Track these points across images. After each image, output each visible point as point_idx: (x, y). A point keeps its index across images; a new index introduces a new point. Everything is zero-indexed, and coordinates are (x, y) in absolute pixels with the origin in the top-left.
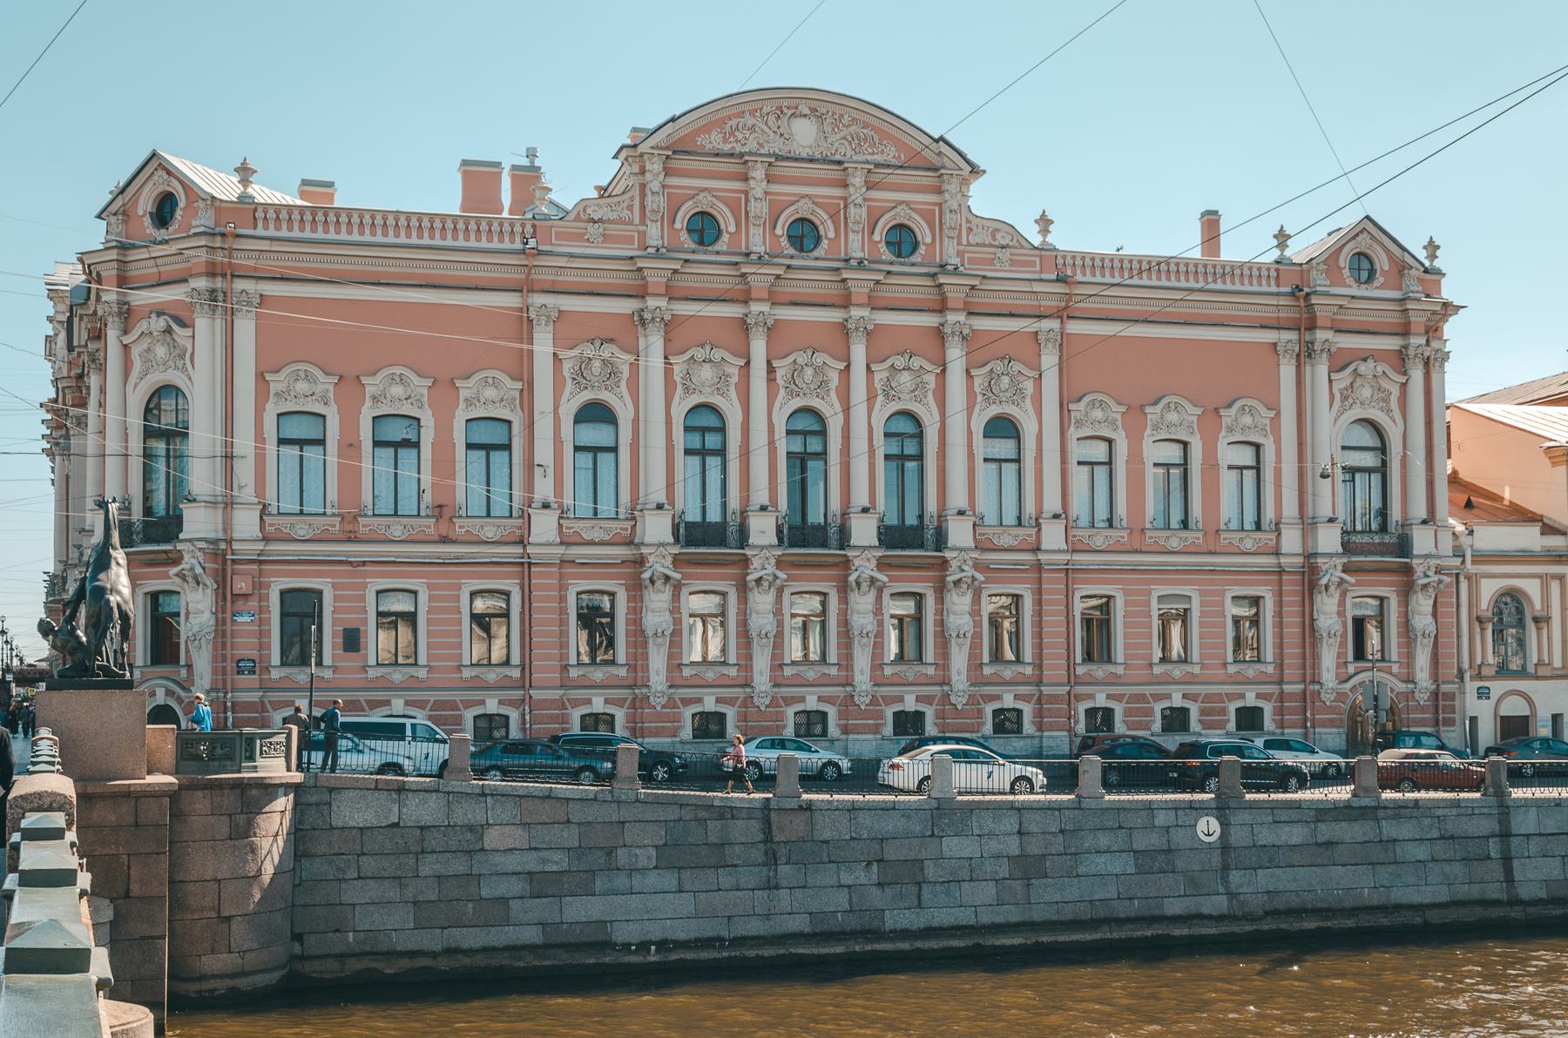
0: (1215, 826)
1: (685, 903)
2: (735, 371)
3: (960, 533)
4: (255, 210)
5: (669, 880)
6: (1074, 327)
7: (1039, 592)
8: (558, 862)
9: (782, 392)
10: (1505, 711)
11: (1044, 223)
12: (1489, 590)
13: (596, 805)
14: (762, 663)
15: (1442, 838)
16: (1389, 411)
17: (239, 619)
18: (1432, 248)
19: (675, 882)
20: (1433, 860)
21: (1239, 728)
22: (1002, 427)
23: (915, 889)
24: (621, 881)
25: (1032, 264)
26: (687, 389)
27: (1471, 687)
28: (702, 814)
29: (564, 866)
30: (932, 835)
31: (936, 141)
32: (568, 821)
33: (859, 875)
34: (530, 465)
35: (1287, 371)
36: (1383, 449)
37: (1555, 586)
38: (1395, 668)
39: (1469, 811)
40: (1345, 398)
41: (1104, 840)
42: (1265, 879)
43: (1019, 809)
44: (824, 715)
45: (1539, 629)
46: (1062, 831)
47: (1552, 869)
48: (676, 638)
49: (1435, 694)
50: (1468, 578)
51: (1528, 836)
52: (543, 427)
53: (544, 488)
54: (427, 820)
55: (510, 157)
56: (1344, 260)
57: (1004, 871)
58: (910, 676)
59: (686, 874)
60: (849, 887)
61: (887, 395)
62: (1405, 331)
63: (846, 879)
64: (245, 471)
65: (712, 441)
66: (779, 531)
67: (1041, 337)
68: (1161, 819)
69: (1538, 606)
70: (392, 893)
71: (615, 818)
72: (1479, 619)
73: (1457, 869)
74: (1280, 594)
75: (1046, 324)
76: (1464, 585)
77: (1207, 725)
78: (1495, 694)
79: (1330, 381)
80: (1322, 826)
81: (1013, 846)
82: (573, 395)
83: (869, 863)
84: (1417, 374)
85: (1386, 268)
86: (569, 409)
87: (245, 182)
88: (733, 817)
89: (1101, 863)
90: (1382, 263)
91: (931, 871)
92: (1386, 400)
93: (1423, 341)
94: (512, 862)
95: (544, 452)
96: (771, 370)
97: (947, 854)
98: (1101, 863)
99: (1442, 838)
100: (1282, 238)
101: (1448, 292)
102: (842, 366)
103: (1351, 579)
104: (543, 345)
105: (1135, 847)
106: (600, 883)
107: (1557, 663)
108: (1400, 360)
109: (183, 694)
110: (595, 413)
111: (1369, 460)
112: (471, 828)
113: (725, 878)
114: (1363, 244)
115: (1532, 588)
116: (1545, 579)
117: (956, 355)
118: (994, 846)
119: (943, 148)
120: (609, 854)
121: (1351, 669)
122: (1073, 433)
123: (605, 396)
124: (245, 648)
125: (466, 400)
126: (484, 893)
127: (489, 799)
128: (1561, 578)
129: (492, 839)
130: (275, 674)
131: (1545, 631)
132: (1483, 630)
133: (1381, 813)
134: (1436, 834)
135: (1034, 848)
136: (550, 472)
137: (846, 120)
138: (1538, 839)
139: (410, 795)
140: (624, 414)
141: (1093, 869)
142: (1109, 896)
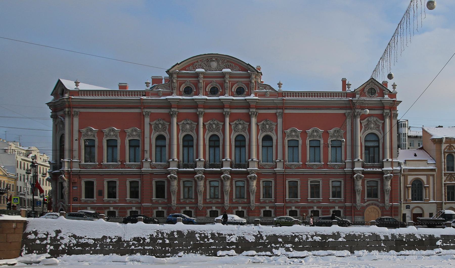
2: (195, 126)
6: (287, 111)
9: (207, 131)
11: (280, 85)
12: (410, 179)
16: (379, 130)
22: (267, 138)
26: (182, 130)
27: (403, 206)
34: (144, 151)
35: (348, 122)
36: (378, 141)
37: (431, 178)
38: (379, 200)
40: (365, 128)
45: (426, 190)
52: (147, 141)
53: (147, 155)
56: (366, 90)
61: (235, 130)
62: (383, 108)
64: (76, 154)
65: (190, 143)
67: (277, 114)
69: (426, 183)
72: (408, 187)
74: (345, 181)
75: (279, 111)
84: (388, 121)
85: (379, 92)
86: (154, 136)
87: (77, 85)
92: (379, 127)
93: (388, 111)
95: (147, 147)
96: (204, 125)
101: (398, 98)
102: (222, 123)
104: (147, 120)
110: (161, 138)
111: (375, 144)
115: (424, 178)
117: (254, 120)
122: (286, 140)
125: (128, 135)
128: (433, 175)
131: (427, 191)
132: (408, 190)
136: (148, 152)
140: (167, 137)
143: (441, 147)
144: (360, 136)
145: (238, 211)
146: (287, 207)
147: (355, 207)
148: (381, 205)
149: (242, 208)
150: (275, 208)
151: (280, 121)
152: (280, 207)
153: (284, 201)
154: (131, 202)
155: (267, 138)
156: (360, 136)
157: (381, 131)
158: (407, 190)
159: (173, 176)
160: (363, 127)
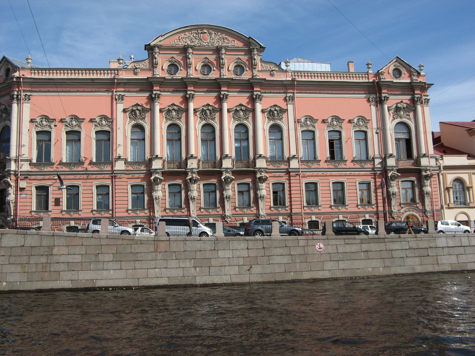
0: (322, 246)
1: (121, 274)
3: (261, 164)
5: (117, 265)
7: (290, 183)
8: (78, 258)
13: (92, 239)
15: (410, 249)
17: (22, 196)
19: (119, 266)
20: (407, 257)
23: (208, 269)
24: (100, 266)
28: (130, 242)
29: (80, 260)
30: (215, 249)
31: (249, 38)
32: (82, 245)
33: (188, 264)
35: (373, 108)
38: (418, 205)
39: (420, 239)
40: (393, 115)
41: (279, 251)
42: (342, 265)
43: (247, 240)
46: (264, 248)
47: (453, 259)
50: (442, 174)
51: (443, 248)
53: (120, 151)
54: (34, 244)
57: (241, 262)
59: (123, 263)
60: (183, 268)
63: (182, 265)
67: (288, 98)
68: (302, 243)
70: (19, 269)
71: (99, 244)
72: (448, 189)
73: (417, 260)
76: (441, 177)
79: (389, 110)
80: (364, 245)
81: (245, 253)
82: (130, 123)
83: (191, 259)
84: (419, 107)
88: (141, 244)
89: (277, 260)
90: (404, 71)
91: (213, 262)
93: (420, 96)
94: (63, 259)
97: (220, 256)
98: (277, 260)
99: (410, 249)
103: (399, 174)
105: (292, 254)
106: (92, 266)
108: (414, 102)
112: (49, 247)
113: (138, 265)
118: (238, 253)
119: (251, 40)
120: (96, 256)
123: (141, 122)
126: (52, 269)
127: (55, 237)
129: (55, 251)
131: (471, 192)
132: (449, 192)
133: (386, 240)
134: (408, 248)
135: (253, 253)
137: (219, 34)
138: (447, 249)
139: (29, 236)
141: (276, 262)
142: (282, 271)
144: (390, 124)
151: (290, 107)
155: (276, 129)
156: (390, 124)
157: (413, 120)
159: (158, 178)
160: (392, 115)
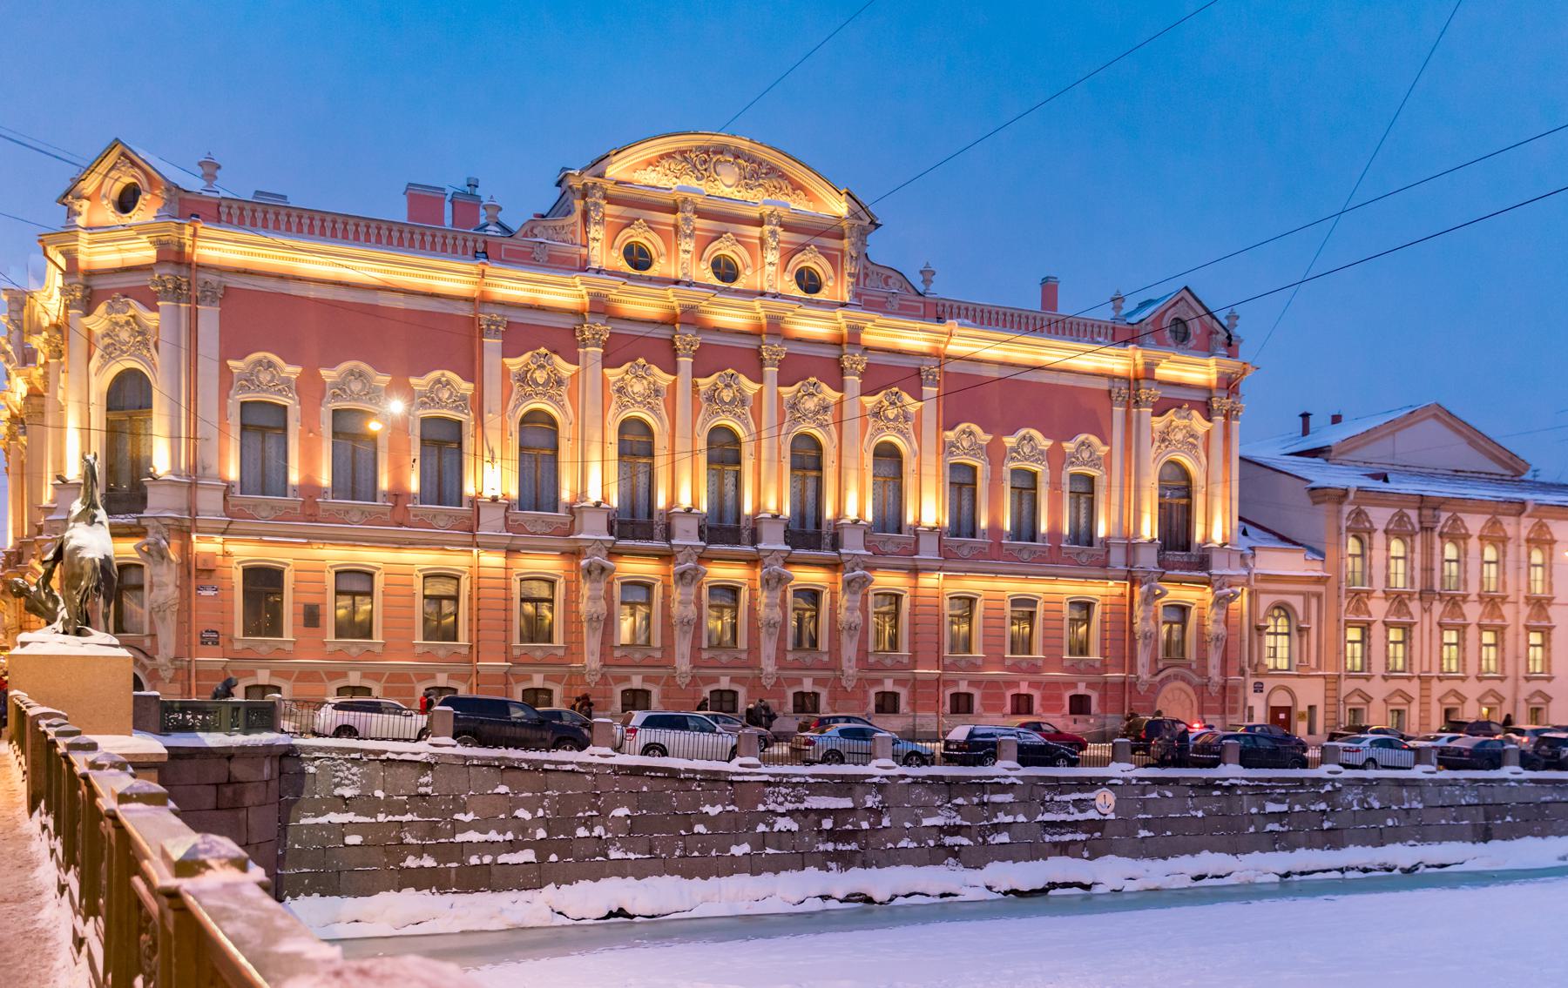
4: (219, 205)
10: (1275, 702)
11: (927, 274)
14: (683, 648)
17: (204, 593)
18: (1233, 317)
21: (1071, 712)
25: (918, 309)
37: (1314, 602)
44: (735, 693)
45: (1301, 636)
48: (608, 624)
49: (1224, 688)
55: (452, 182)
58: (808, 660)
66: (701, 531)
77: (1046, 708)
78: (1266, 690)
100: (1117, 300)
107: (1313, 664)
109: (146, 661)
114: (1181, 312)
116: (1306, 596)
121: (1160, 666)
124: (203, 619)
128: (1319, 596)
130: (238, 646)
143: (1339, 512)
145: (802, 693)
146: (947, 683)
147: (1133, 685)
148: (1197, 680)
149: (816, 682)
150: (916, 685)
152: (926, 683)
153: (939, 661)
154: (427, 655)
158: (1255, 636)
